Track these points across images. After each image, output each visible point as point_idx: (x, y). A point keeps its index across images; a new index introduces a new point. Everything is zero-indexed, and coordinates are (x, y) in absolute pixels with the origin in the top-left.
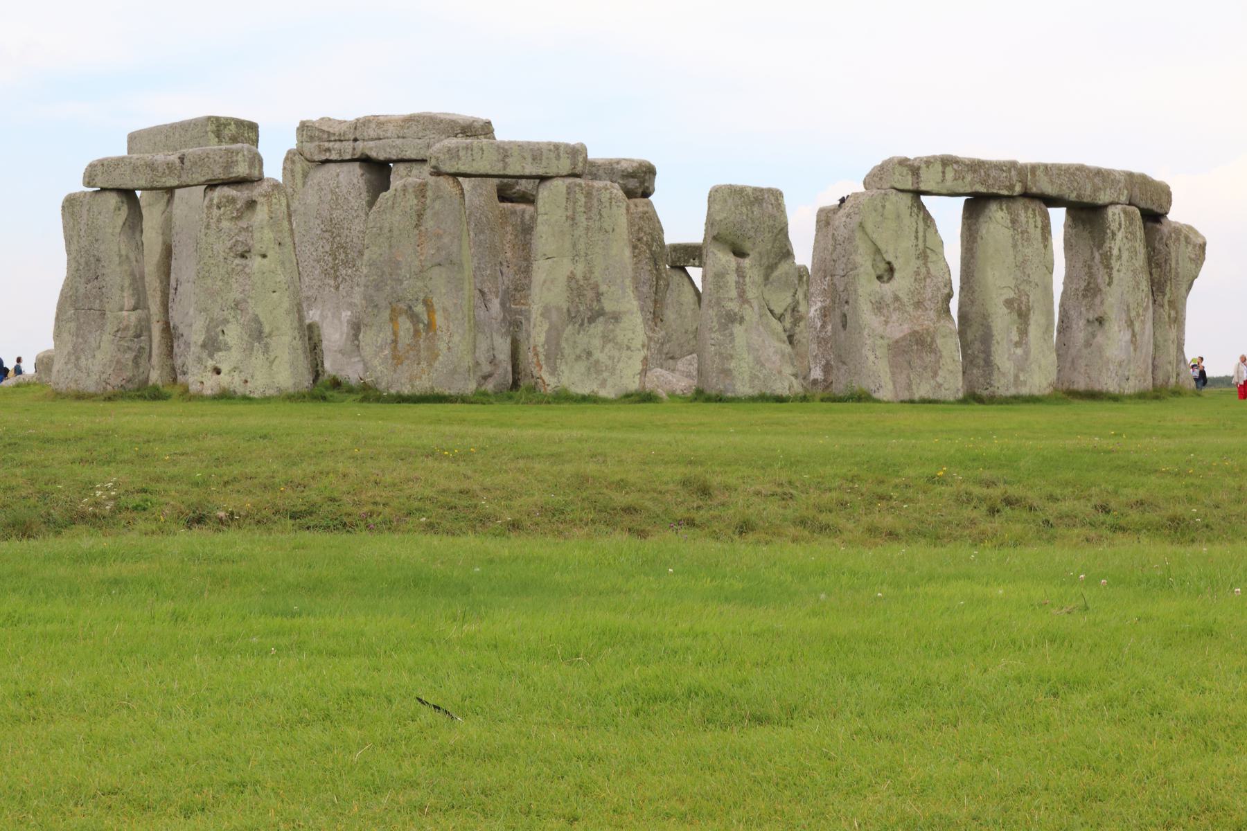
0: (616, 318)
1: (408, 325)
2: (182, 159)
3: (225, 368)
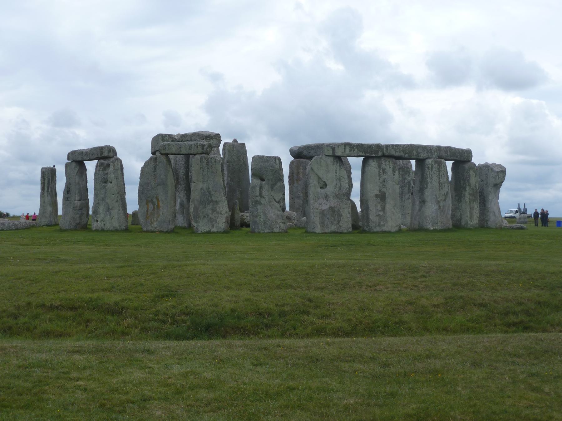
1: (152, 206)
3: (99, 220)
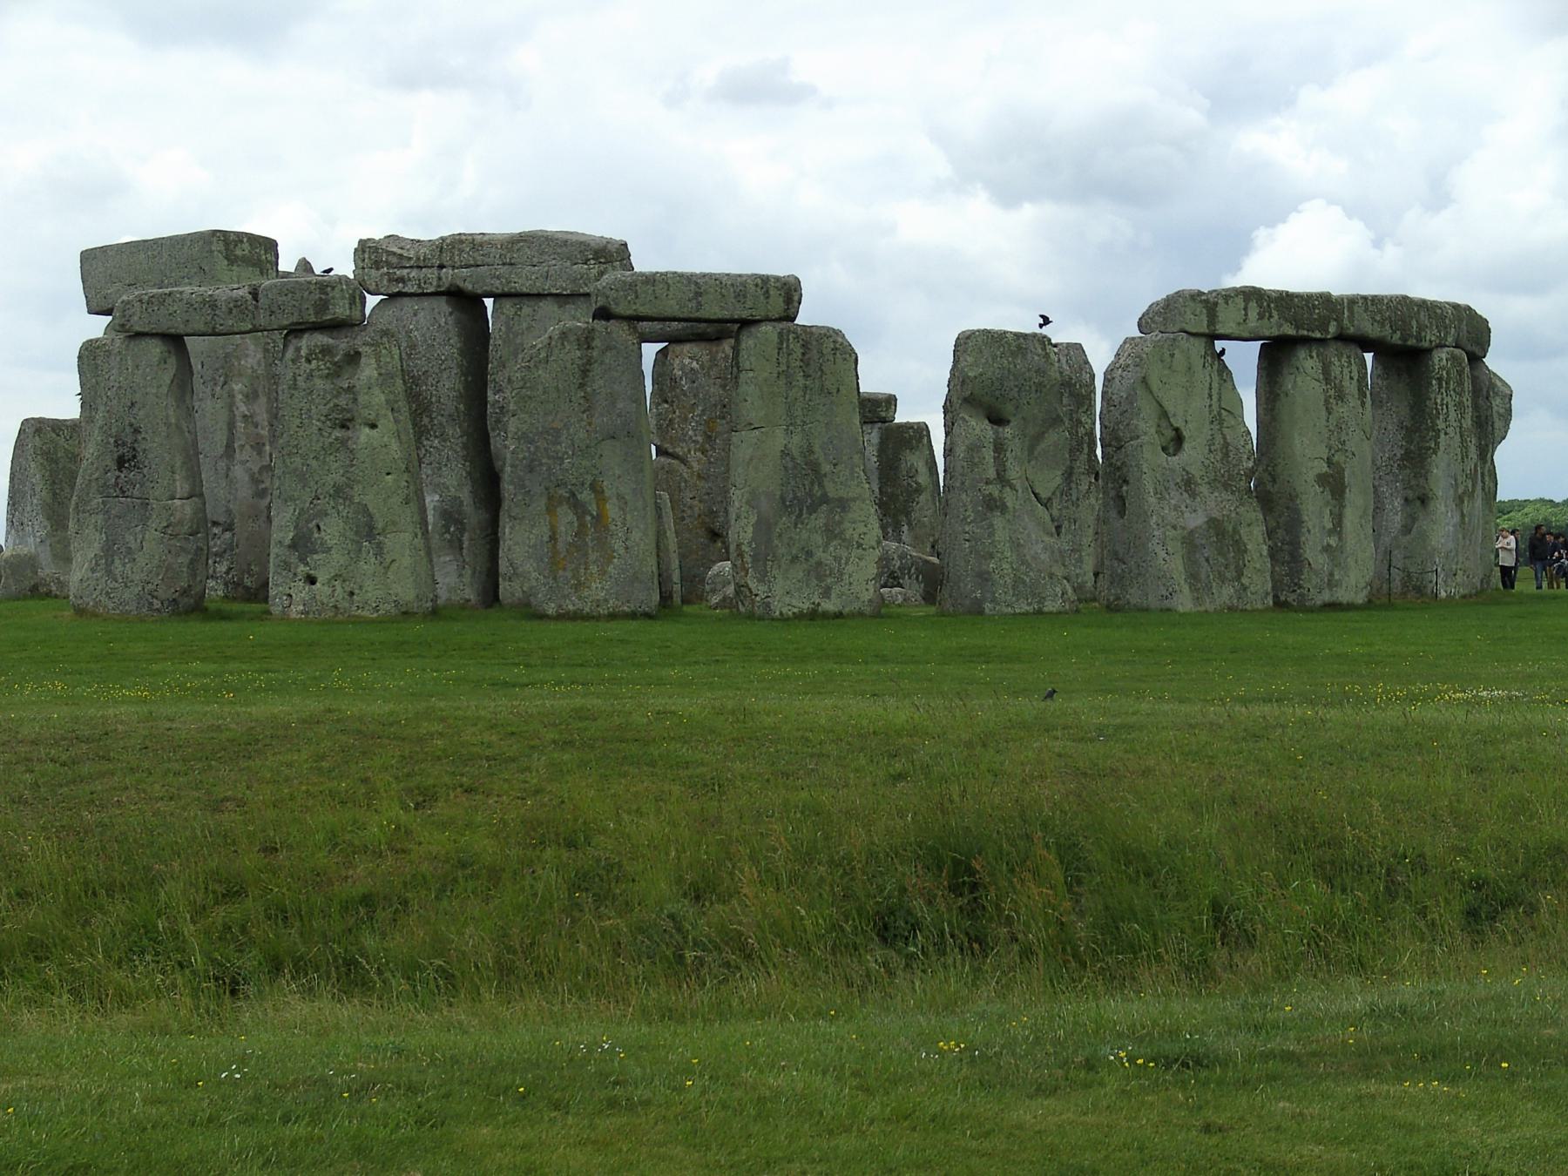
0: (843, 504)
1: (571, 517)
2: (255, 294)
3: (322, 577)
